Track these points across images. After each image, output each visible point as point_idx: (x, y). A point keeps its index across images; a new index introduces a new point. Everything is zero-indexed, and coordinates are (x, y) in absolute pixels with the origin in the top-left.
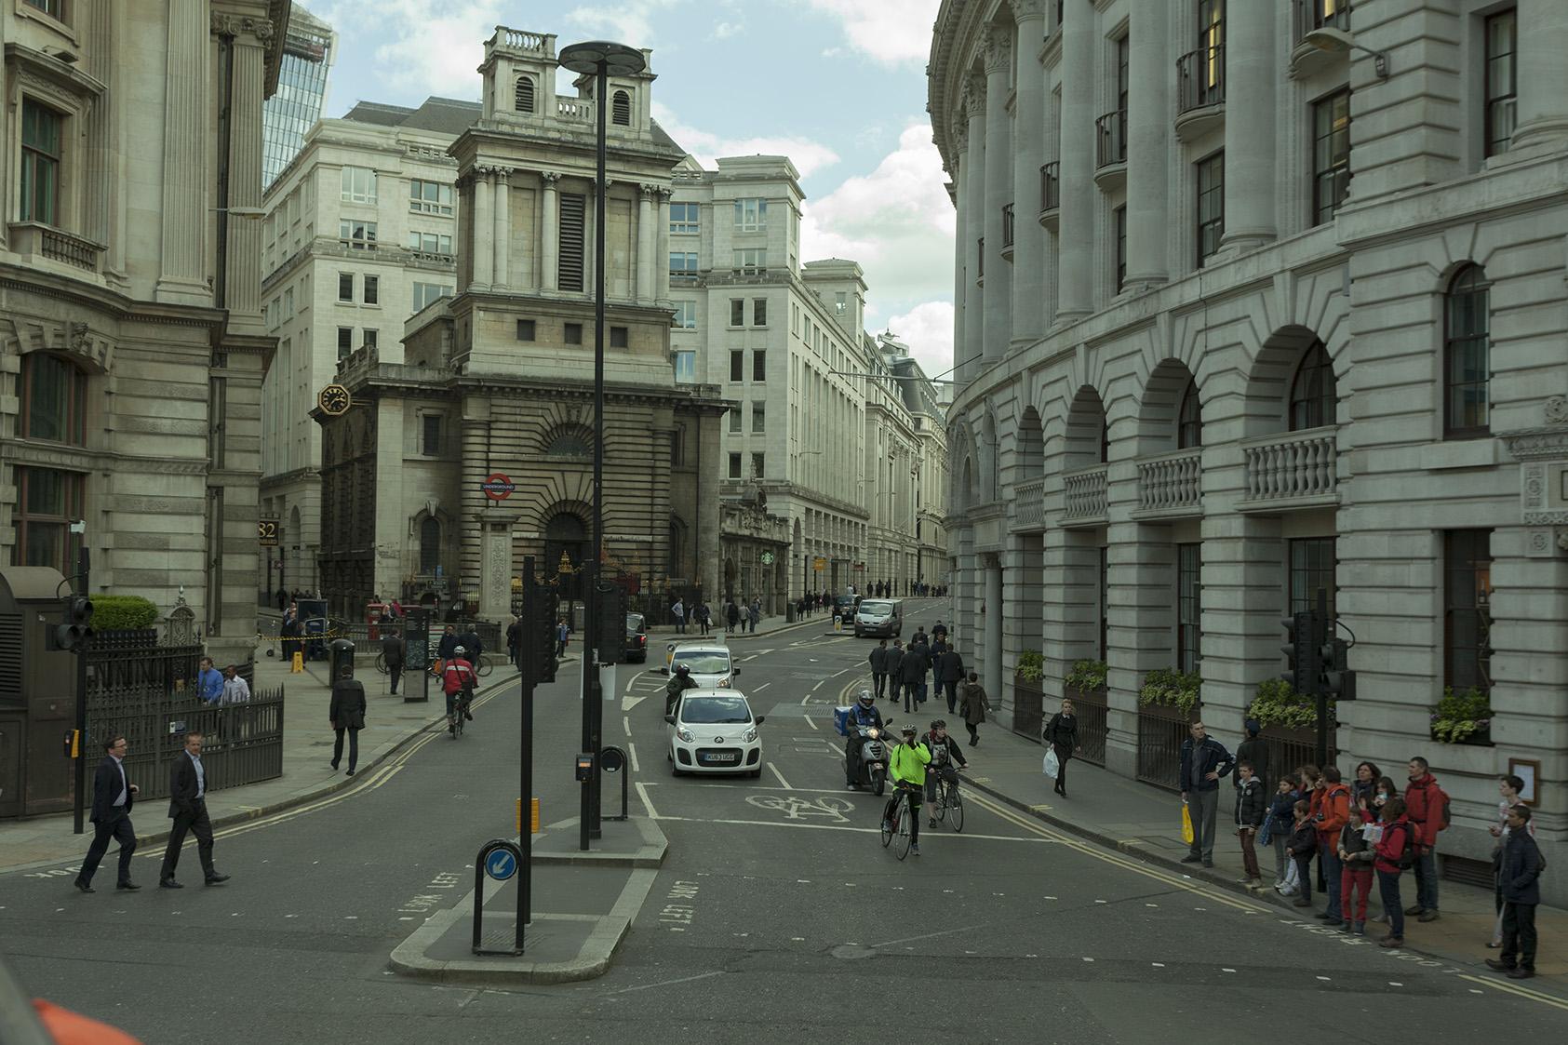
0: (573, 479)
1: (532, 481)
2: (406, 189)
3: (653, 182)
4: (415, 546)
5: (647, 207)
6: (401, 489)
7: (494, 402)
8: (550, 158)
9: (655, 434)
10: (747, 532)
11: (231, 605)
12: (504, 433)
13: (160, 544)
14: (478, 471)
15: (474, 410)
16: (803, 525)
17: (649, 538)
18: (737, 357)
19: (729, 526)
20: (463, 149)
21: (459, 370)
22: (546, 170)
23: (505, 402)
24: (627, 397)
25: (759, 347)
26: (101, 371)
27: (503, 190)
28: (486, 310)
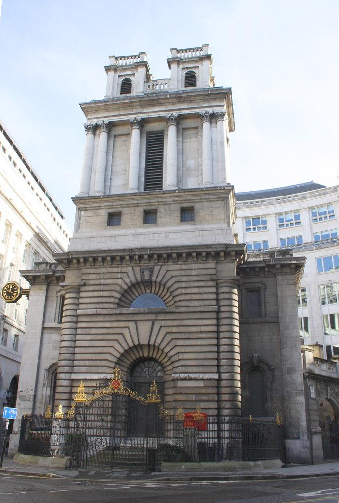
0: (145, 327)
1: (111, 331)
3: (210, 110)
5: (206, 125)
7: (84, 271)
12: (90, 294)
14: (68, 325)
17: (216, 376)
23: (92, 270)
24: (189, 255)
27: (103, 136)
28: (85, 209)
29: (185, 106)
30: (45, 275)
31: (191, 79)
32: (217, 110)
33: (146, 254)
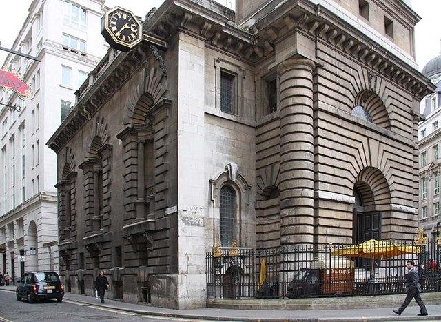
4: (216, 213)
6: (202, 148)
7: (320, 45)
30: (212, 23)
33: (382, 57)
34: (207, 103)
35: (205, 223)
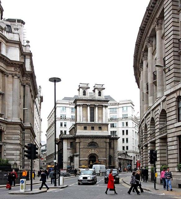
0: (93, 150)
2: (71, 109)
5: (104, 108)
8: (88, 102)
9: (106, 143)
10: (124, 158)
11: (26, 164)
13: (13, 155)
15: (77, 140)
16: (135, 157)
18: (123, 131)
19: (120, 157)
20: (75, 101)
21: (75, 135)
22: (88, 104)
24: (102, 137)
25: (127, 129)
26: (4, 131)
27: (81, 107)
28: (79, 125)
29: (99, 102)
31: (100, 94)
32: (106, 105)
34: (68, 147)
35: (67, 163)
